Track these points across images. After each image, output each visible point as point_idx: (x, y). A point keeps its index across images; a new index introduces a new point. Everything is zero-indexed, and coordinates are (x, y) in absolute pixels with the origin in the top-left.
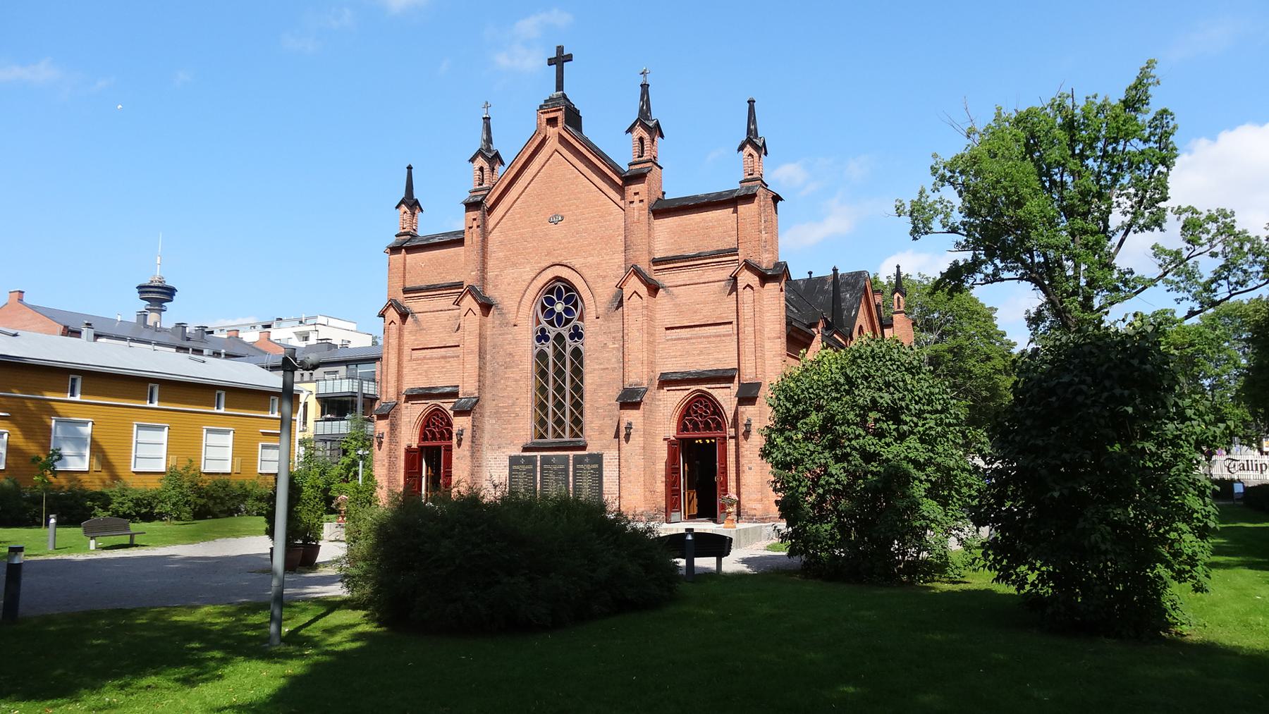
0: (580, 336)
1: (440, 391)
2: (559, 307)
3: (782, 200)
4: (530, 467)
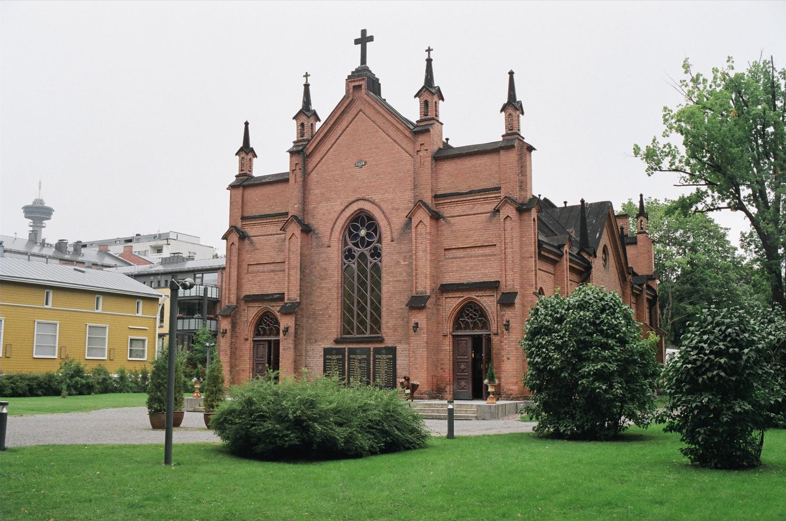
0: (379, 255)
1: (270, 297)
2: (363, 233)
3: (535, 149)
4: (340, 357)
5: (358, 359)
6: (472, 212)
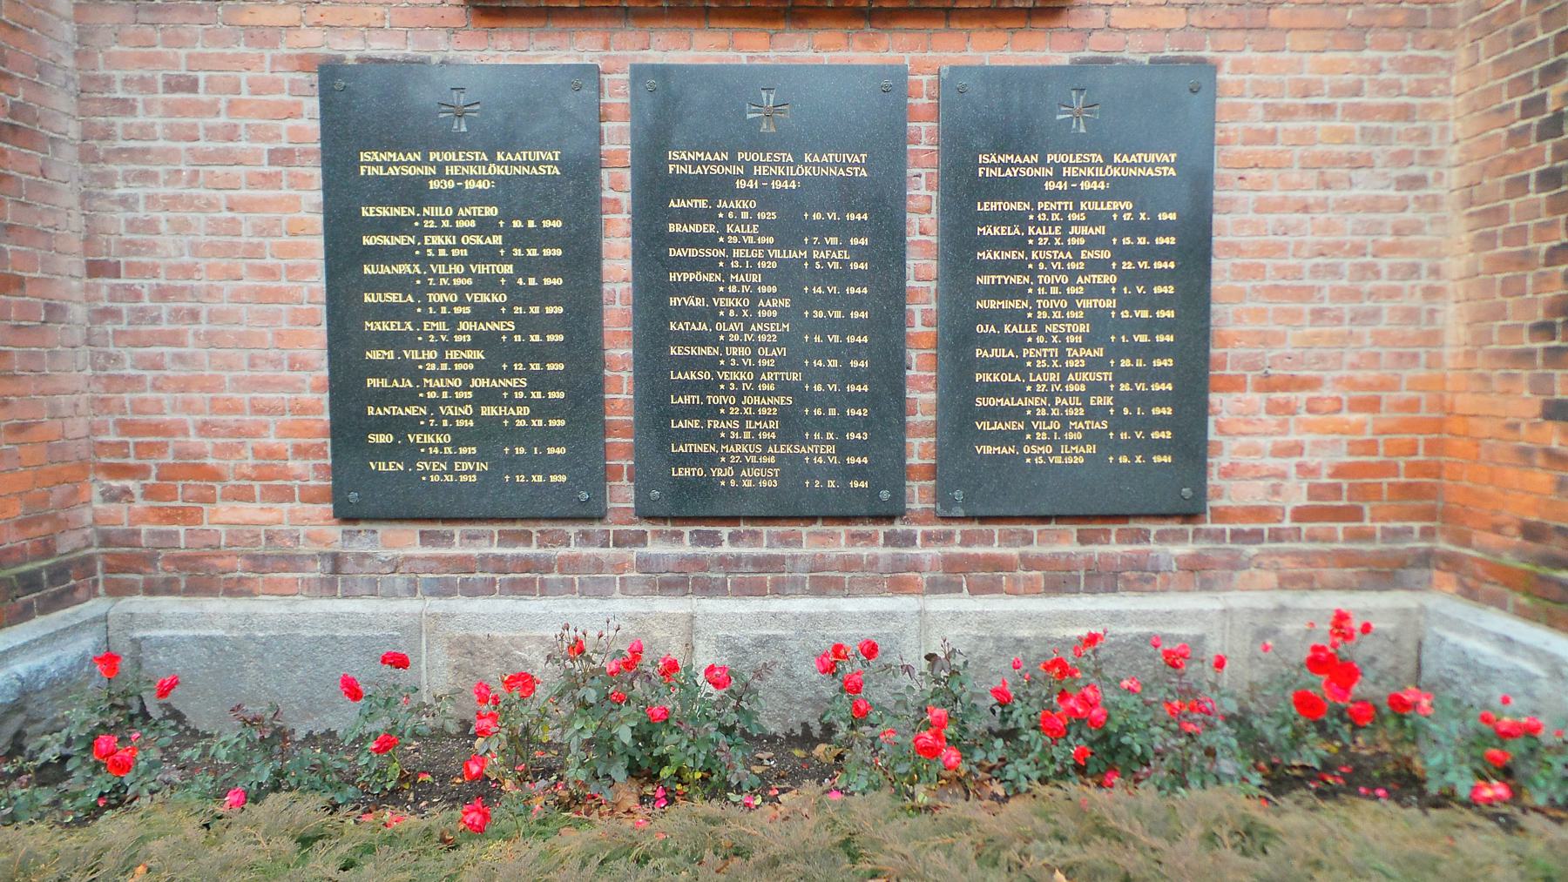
5: (766, 197)
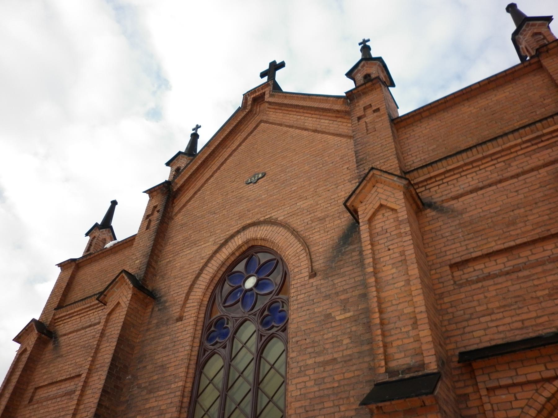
6: (509, 174)
